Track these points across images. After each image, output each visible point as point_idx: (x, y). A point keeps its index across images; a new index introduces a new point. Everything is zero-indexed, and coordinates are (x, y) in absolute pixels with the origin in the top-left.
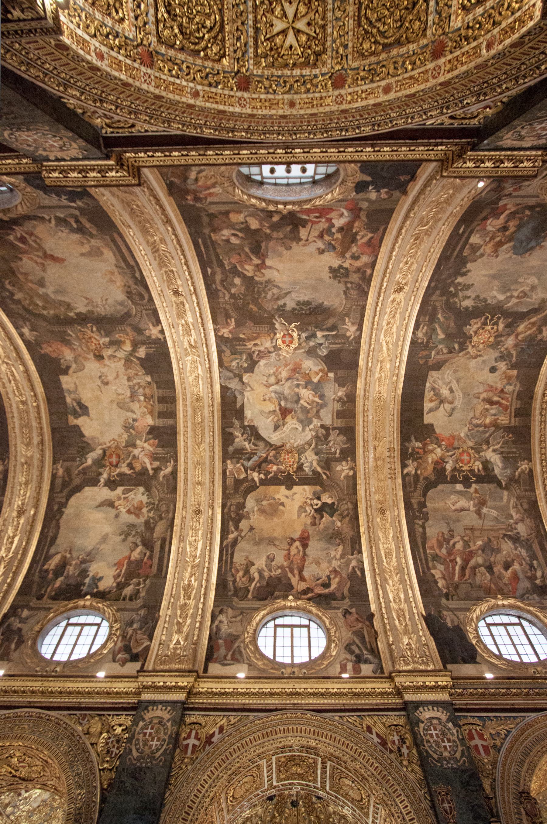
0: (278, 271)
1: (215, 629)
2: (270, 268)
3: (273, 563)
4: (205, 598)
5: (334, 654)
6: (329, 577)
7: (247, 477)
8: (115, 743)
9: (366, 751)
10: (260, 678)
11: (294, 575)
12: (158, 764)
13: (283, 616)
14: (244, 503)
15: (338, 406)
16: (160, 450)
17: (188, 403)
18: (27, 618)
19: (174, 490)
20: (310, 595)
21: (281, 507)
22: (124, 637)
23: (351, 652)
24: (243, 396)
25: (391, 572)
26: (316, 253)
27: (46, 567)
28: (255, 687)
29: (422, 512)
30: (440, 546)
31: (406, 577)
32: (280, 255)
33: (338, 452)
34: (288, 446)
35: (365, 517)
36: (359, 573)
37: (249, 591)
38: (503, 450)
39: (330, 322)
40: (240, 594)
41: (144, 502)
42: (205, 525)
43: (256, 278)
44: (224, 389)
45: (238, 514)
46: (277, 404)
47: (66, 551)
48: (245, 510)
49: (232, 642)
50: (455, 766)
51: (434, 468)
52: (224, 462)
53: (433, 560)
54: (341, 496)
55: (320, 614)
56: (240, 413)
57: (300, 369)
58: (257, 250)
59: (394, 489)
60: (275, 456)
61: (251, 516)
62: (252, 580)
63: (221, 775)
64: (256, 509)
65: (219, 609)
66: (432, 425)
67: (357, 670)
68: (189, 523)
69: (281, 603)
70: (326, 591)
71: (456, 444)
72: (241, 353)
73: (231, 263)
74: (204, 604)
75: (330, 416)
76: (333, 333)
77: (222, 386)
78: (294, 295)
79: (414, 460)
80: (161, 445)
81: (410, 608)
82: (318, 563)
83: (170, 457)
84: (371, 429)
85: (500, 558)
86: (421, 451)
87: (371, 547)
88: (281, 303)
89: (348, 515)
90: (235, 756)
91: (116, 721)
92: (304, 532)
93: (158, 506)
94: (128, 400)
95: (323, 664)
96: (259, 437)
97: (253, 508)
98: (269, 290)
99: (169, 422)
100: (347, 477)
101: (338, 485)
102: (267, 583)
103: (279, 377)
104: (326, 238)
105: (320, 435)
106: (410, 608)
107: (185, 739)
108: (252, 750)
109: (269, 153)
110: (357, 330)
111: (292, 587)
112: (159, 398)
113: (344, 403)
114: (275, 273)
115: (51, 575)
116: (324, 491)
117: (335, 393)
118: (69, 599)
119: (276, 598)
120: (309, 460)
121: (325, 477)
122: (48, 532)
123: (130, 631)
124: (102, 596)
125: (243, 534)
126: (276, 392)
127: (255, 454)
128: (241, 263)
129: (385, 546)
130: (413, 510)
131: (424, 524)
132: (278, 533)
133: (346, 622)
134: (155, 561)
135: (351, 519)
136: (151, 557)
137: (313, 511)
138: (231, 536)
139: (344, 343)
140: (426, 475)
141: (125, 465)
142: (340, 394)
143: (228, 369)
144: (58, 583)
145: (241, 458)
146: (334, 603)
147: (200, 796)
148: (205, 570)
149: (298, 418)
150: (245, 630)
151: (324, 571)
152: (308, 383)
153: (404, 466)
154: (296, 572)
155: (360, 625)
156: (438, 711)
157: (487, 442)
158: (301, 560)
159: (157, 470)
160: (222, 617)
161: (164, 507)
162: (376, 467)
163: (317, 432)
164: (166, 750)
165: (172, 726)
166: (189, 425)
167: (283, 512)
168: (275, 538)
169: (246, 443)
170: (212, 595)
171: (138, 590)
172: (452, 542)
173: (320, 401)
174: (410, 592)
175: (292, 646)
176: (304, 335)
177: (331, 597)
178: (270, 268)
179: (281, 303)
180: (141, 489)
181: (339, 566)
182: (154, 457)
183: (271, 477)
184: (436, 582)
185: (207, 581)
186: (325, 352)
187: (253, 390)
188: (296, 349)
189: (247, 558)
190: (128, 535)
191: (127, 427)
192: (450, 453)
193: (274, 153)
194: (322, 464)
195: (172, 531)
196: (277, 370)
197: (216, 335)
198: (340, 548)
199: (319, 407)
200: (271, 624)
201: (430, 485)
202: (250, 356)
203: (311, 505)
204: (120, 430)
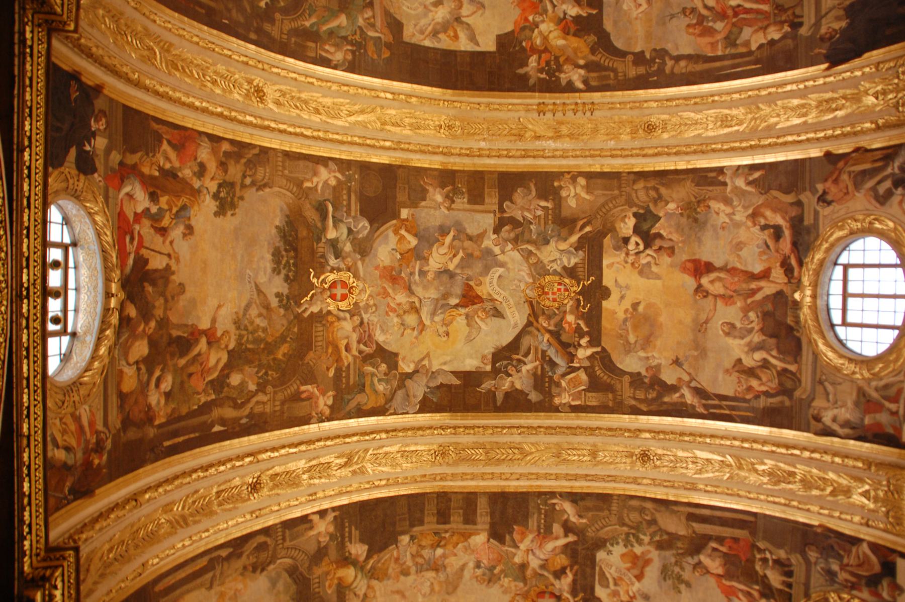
0: (219, 307)
1: (847, 431)
2: (214, 321)
3: (738, 325)
4: (794, 447)
5: (891, 224)
6: (764, 228)
7: (585, 368)
11: (760, 289)
14: (631, 374)
15: (461, 202)
16: (533, 523)
17: (449, 470)
19: (605, 499)
20: (793, 262)
21: (641, 308)
23: (889, 194)
24: (439, 372)
25: (756, 119)
26: (192, 240)
29: (653, 60)
30: (710, 32)
31: (764, 93)
32: (193, 302)
33: (543, 203)
34: (531, 294)
35: (659, 159)
36: (757, 175)
37: (785, 370)
39: (311, 215)
40: (789, 384)
41: (624, 550)
42: (667, 444)
43: (231, 347)
44: (425, 406)
45: (651, 386)
46: (455, 312)
48: (644, 373)
51: (575, 35)
52: (556, 410)
53: (734, 45)
55: (825, 245)
56: (470, 379)
57: (393, 268)
58: (184, 345)
59: (611, 106)
60: (549, 318)
61: (654, 363)
62: (765, 364)
64: (642, 354)
65: (813, 422)
66: (499, 38)
68: (663, 473)
69: (805, 313)
70: (787, 233)
72: (362, 375)
73: (204, 390)
74: (804, 449)
75: (478, 216)
76: (330, 208)
77: (420, 411)
78: (262, 279)
79: (559, 69)
80: (523, 520)
81: (816, 89)
82: (739, 246)
83: (546, 504)
84: (502, 144)
87: (714, 150)
88: (274, 302)
89: (656, 190)
92: (684, 269)
93: (632, 528)
94: (442, 576)
96: (514, 345)
97: (640, 359)
98: (252, 323)
99: (483, 505)
100: (588, 189)
101: (603, 205)
102: (771, 336)
103: (406, 307)
104: (166, 222)
105: (512, 235)
106: (816, 89)
109: (27, 327)
110: (326, 166)
111: (780, 294)
112: (438, 523)
113: (456, 191)
114: (223, 312)
116: (613, 230)
117: (438, 206)
119: (797, 321)
120: (557, 255)
121: (588, 229)
126: (434, 314)
127: (544, 352)
128: (205, 372)
129: (711, 126)
130: (649, 75)
131: (672, 58)
132: (686, 315)
133: (839, 201)
135: (663, 185)
137: (648, 252)
139: (349, 189)
140: (586, 51)
141: (557, 583)
142: (439, 198)
143: (390, 399)
145: (551, 378)
146: (808, 221)
148: (746, 445)
149: (481, 274)
150: (850, 378)
151: (754, 236)
152: (418, 255)
153: (570, 88)
154: (753, 285)
155: (845, 177)
158: (733, 275)
159: (568, 528)
160: (827, 418)
161: (635, 516)
162: (571, 136)
163: (506, 240)
166: (488, 469)
167: (649, 306)
168: (695, 320)
169: (524, 369)
170: (788, 434)
172: (705, 12)
173: (452, 234)
174: (789, 88)
175: (878, 296)
176: (333, 261)
177: (797, 224)
178: (214, 321)
179: (274, 302)
180: (601, 555)
181: (745, 208)
182: (545, 533)
183: (587, 325)
184: (772, 43)
185: (765, 442)
186: (364, 224)
187: (428, 355)
188: (356, 276)
189: (727, 371)
191: (491, 578)
192: (549, 7)
193: (28, 319)
194: (564, 232)
195: (676, 503)
196: (394, 310)
197: (329, 419)
198: (715, 205)
199: (462, 236)
200: (841, 331)
201: (604, 43)
202: (366, 358)
204: (495, 590)
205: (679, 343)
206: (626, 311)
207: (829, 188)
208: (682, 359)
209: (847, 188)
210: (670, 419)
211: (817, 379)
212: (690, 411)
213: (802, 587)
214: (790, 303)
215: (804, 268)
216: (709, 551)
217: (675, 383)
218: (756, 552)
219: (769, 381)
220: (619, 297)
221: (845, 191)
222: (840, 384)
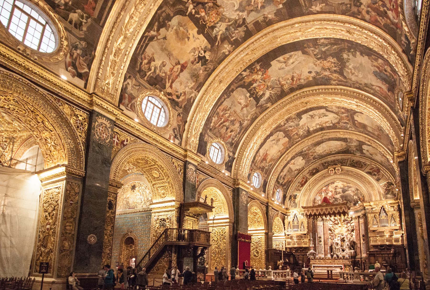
21: (186, 39)
38: (272, 95)
45: (164, 21)
54: (213, 60)
61: (170, 29)
64: (175, 28)
71: (266, 80)
79: (250, 72)
85: (232, 128)
86: (256, 71)
92: (186, 63)
97: (174, 26)
100: (224, 53)
116: (210, 51)
121: (217, 44)
125: (159, 37)
135: (207, 74)
137: (197, 56)
138: (153, 33)
157: (273, 89)
167: (185, 43)
192: (261, 81)
203: (200, 52)
205: (170, 44)
206: (189, 35)
208: (165, 40)
210: (150, 19)
212: (149, 30)
217: (160, 31)
220: (195, 36)
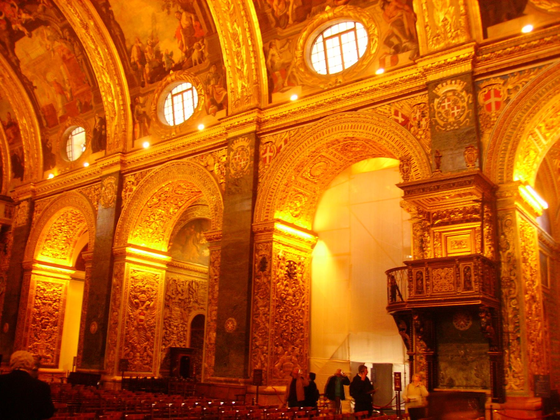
8: (223, 167)
9: (390, 131)
10: (310, 95)
12: (247, 174)
13: (330, 27)
18: (145, 102)
22: (208, 94)
27: (132, 61)
28: (304, 104)
37: (288, 17)
40: (282, 22)
47: (136, 42)
49: (286, 70)
50: (457, 128)
63: (288, 171)
65: (268, 44)
67: (394, 61)
90: (296, 157)
91: (220, 154)
95: (363, 65)
107: (264, 154)
108: (307, 150)
115: (139, 66)
118: (160, 79)
119: (314, 14)
122: (115, 33)
123: (210, 87)
124: (179, 67)
133: (385, 14)
134: (202, 21)
136: (197, 19)
144: (147, 70)
147: (277, 185)
155: (399, 13)
156: (455, 83)
160: (273, 51)
164: (250, 165)
165: (251, 149)
171: (202, 52)
190: (168, 7)
200: (320, 39)
207: (392, 5)
209: (393, 17)
211: (289, 38)
213: (197, 71)
214: (323, 5)
215: (343, 7)
216: (189, 16)
218: (201, 40)
219: (280, 9)
221: (391, 16)
222: (290, 51)
